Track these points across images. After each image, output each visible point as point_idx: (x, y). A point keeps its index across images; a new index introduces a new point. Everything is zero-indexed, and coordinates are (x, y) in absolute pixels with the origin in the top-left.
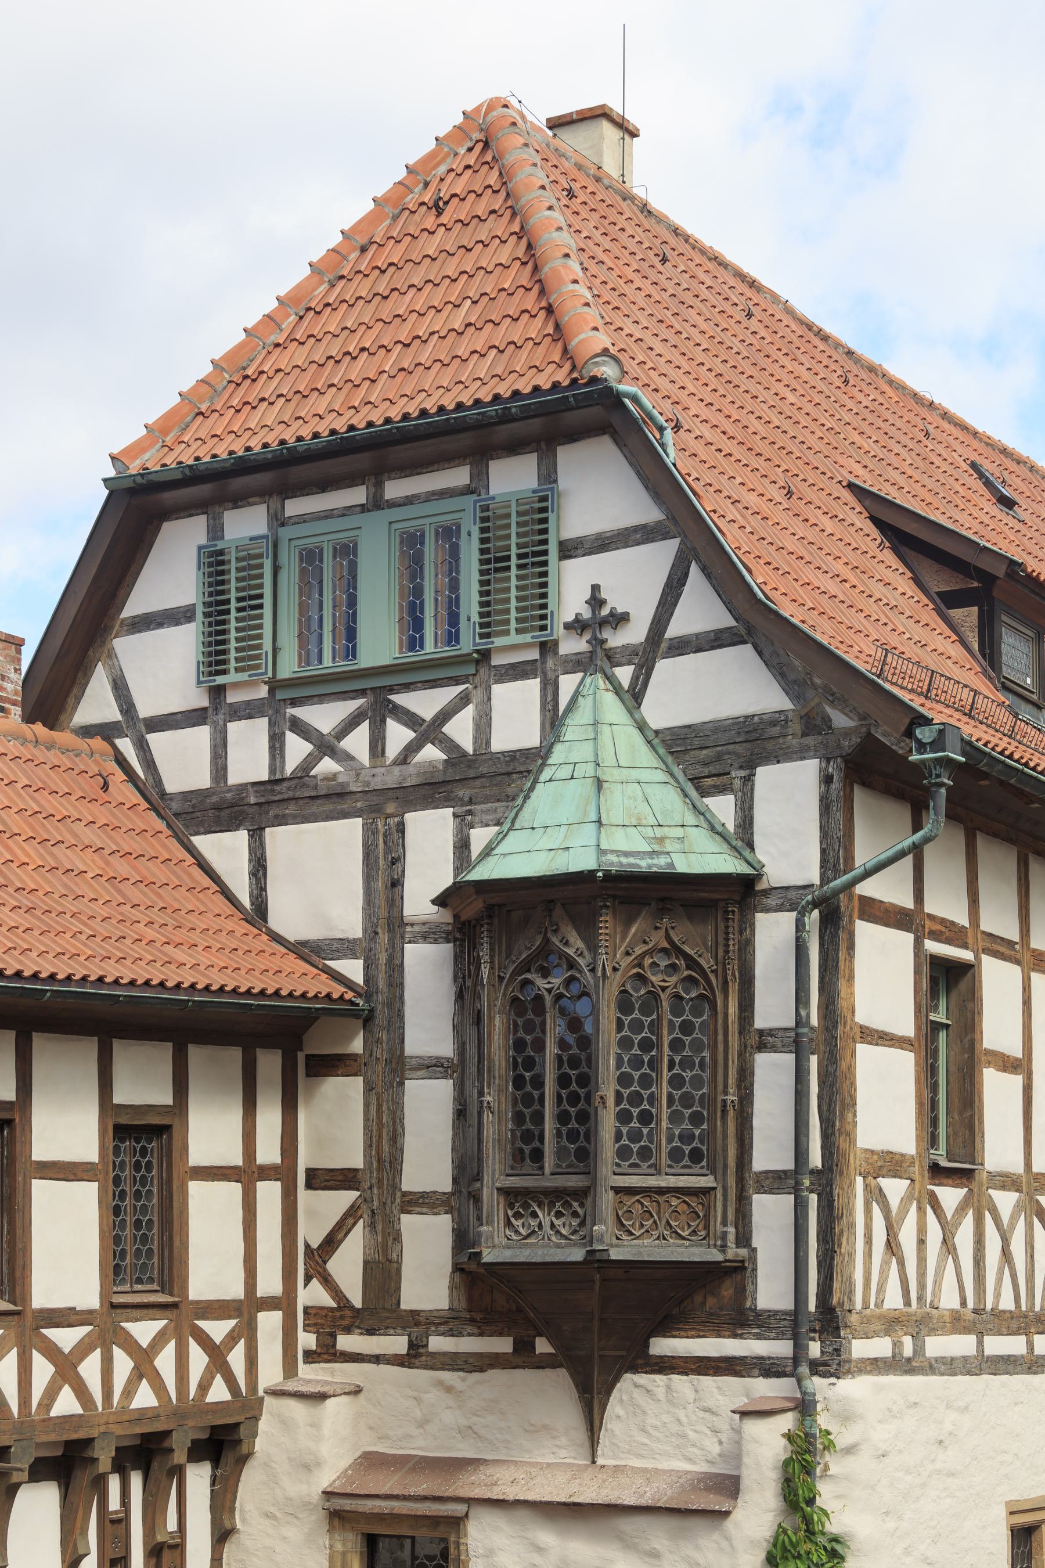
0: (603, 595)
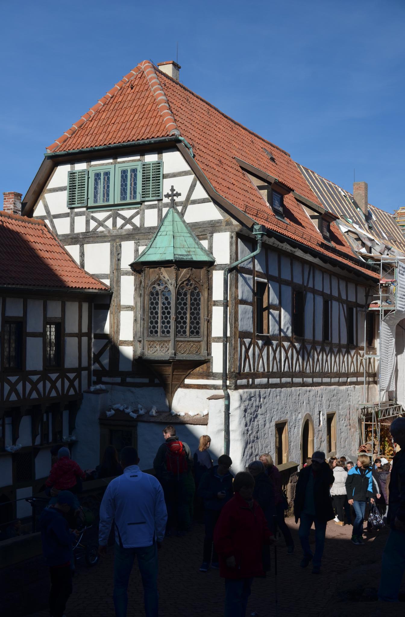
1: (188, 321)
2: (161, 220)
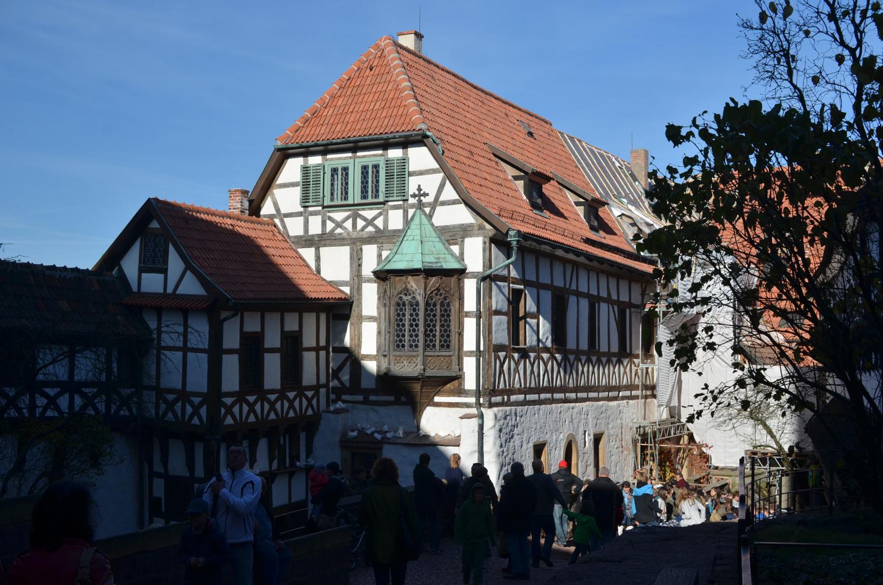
1: (438, 334)
2: (407, 222)
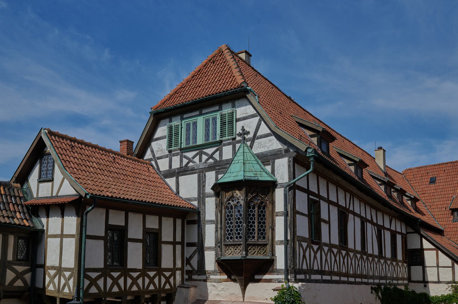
0: (245, 128)
1: (256, 229)
